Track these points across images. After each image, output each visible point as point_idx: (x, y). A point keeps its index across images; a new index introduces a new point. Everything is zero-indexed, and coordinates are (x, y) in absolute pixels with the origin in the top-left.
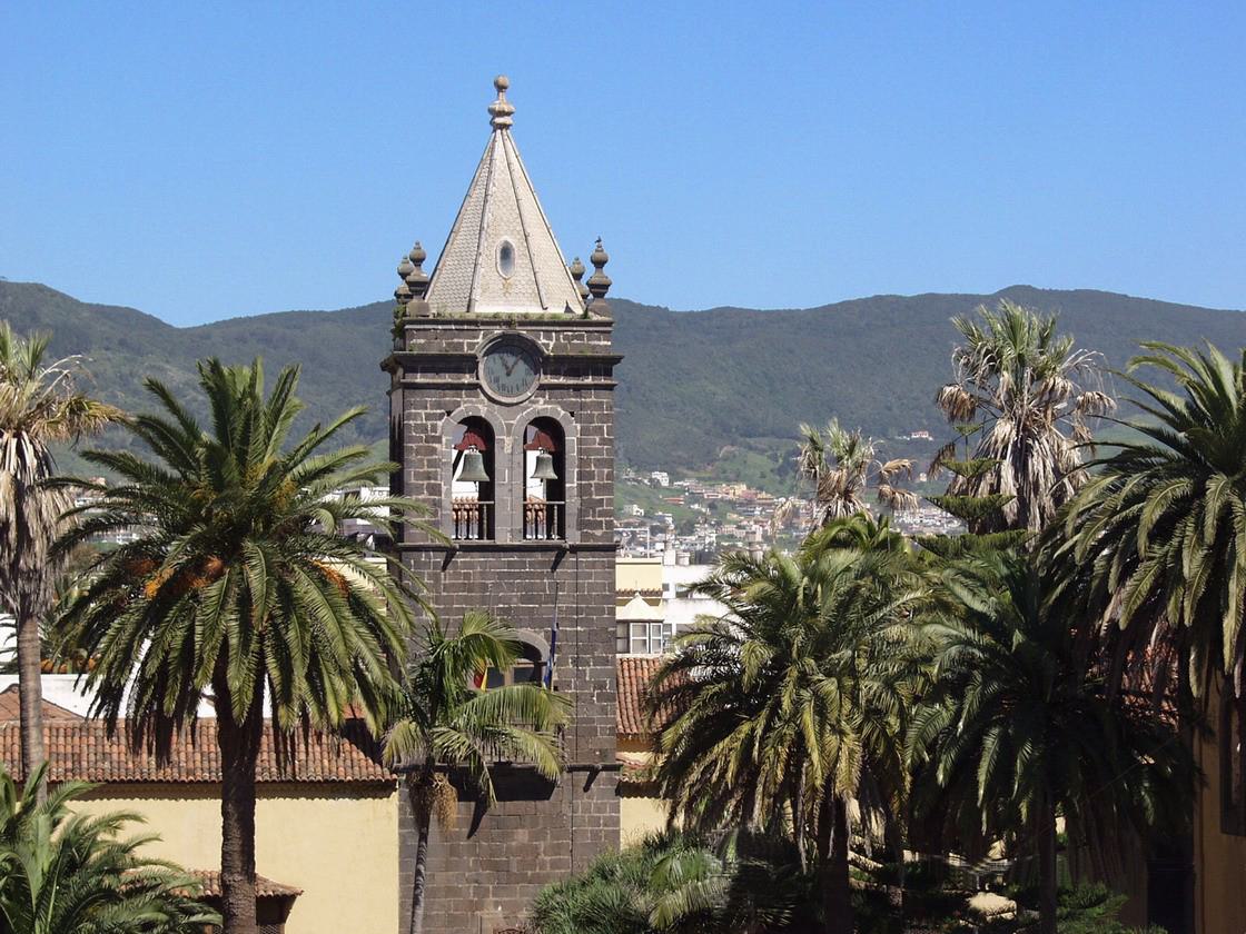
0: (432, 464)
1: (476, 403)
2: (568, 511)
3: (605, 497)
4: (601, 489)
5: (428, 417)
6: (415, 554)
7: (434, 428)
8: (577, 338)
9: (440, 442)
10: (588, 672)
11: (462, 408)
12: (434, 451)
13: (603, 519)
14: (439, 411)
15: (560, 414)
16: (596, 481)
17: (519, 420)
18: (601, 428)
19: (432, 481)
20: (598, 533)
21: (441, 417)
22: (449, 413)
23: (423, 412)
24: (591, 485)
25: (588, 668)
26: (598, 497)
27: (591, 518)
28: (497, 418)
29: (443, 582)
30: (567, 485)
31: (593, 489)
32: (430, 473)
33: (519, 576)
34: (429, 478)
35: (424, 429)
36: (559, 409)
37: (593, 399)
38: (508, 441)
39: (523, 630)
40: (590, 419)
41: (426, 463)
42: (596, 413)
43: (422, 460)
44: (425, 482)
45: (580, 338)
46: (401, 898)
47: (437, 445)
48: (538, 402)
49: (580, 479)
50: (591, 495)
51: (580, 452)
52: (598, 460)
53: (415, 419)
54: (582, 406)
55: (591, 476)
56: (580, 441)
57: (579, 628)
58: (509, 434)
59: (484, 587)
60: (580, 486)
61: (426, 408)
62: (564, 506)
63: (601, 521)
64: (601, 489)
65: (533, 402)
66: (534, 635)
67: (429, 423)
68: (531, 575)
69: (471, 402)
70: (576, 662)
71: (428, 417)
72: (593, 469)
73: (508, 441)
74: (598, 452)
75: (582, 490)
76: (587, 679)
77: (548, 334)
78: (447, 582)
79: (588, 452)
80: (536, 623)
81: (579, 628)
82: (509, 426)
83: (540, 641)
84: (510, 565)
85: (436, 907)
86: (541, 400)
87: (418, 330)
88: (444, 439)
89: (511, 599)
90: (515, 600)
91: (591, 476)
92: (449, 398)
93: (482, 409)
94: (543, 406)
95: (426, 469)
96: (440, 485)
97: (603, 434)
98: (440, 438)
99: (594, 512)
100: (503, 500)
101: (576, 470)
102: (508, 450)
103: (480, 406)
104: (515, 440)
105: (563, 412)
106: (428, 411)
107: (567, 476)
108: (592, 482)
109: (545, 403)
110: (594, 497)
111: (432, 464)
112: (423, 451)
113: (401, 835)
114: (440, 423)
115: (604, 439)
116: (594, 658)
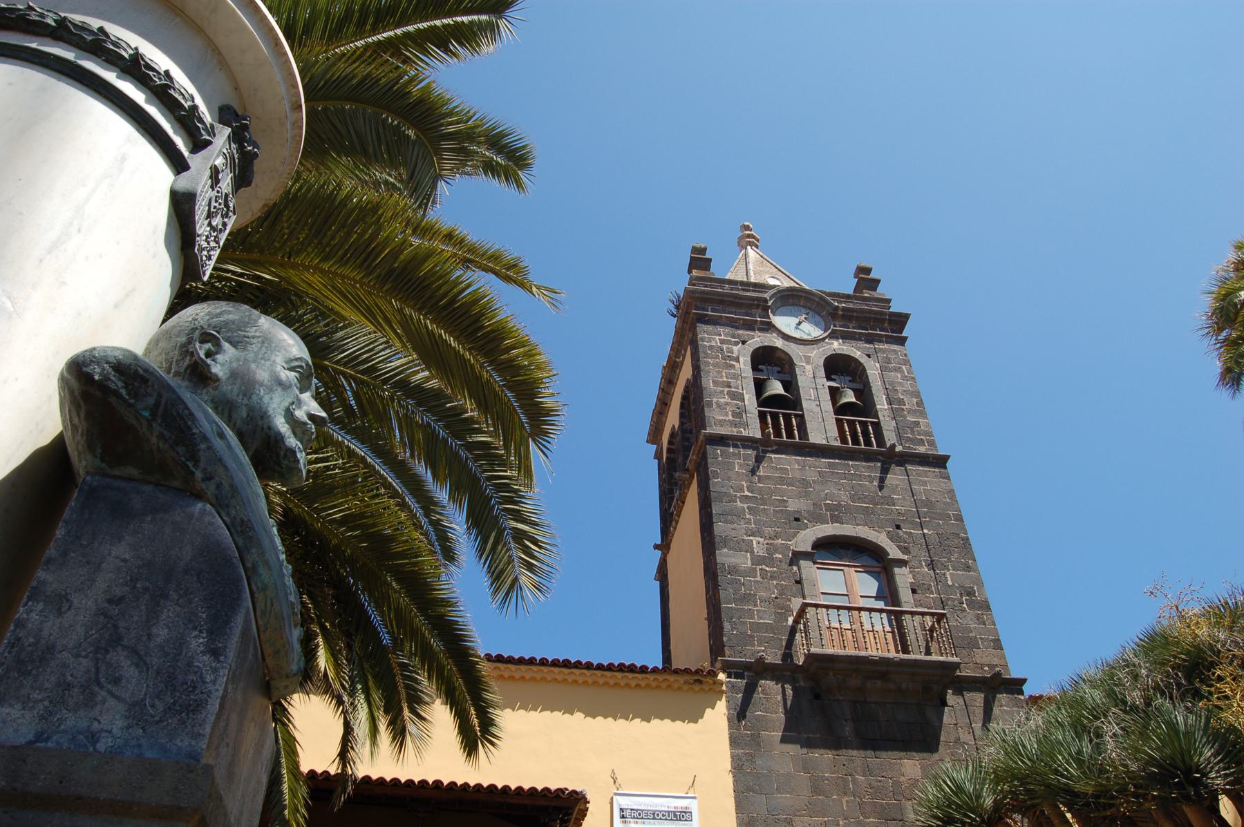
5: (722, 342)
15: (857, 354)
17: (818, 355)
21: (736, 344)
22: (744, 342)
28: (794, 350)
33: (845, 476)
34: (730, 387)
38: (809, 368)
49: (890, 403)
55: (901, 402)
58: (808, 363)
59: (805, 483)
70: (932, 565)
75: (895, 414)
79: (892, 383)
83: (881, 539)
88: (741, 359)
93: (779, 343)
94: (837, 346)
114: (735, 349)
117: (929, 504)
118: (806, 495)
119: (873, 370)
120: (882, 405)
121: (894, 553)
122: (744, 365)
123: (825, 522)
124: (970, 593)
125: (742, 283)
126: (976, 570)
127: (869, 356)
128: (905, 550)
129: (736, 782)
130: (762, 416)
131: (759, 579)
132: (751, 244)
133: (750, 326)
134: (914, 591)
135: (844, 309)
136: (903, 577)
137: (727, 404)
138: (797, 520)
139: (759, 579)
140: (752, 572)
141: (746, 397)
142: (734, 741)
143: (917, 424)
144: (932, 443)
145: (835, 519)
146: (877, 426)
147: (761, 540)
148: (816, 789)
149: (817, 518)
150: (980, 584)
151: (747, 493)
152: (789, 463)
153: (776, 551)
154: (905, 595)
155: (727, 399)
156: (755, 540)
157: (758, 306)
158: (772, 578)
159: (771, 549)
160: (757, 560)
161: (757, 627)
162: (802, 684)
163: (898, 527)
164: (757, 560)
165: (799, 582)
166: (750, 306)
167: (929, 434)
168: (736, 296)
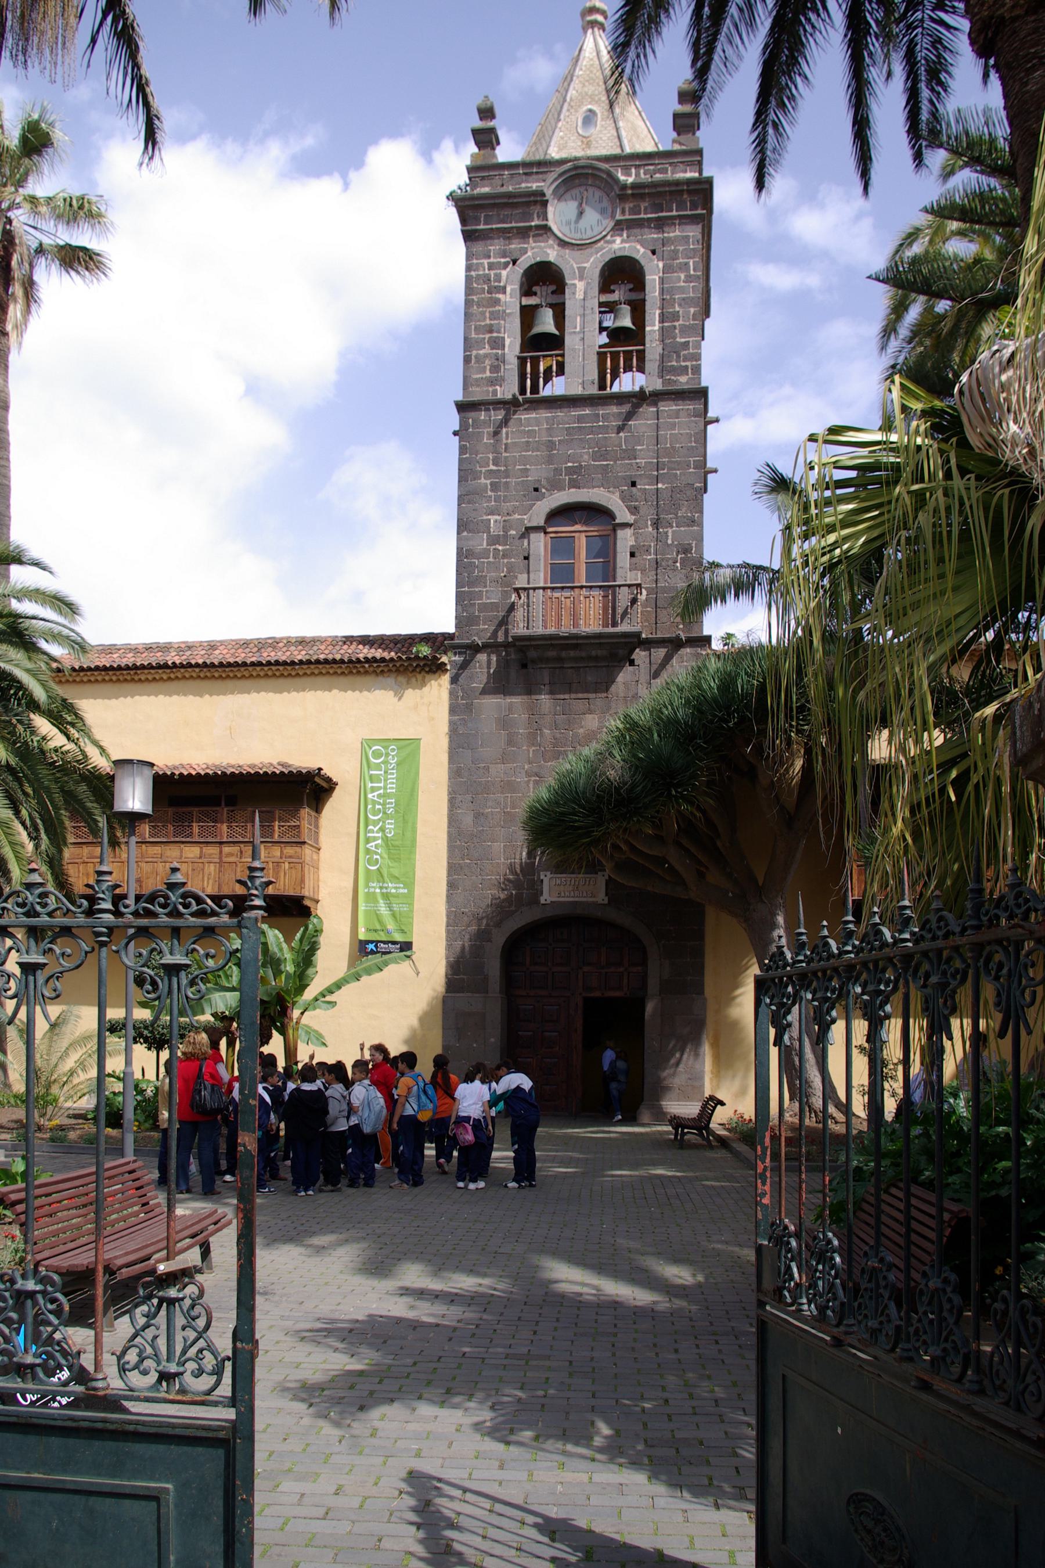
0: (494, 316)
1: (545, 247)
2: (648, 356)
3: (691, 339)
4: (685, 330)
6: (473, 414)
7: (498, 278)
8: (660, 171)
9: (505, 293)
10: (670, 534)
11: (529, 254)
12: (497, 302)
13: (688, 364)
14: (503, 260)
15: (639, 252)
16: (681, 322)
17: (594, 262)
18: (687, 264)
19: (495, 335)
20: (683, 379)
21: (506, 265)
22: (514, 262)
23: (485, 262)
24: (675, 327)
25: (670, 531)
26: (683, 340)
27: (674, 363)
29: (504, 441)
30: (648, 329)
31: (677, 331)
32: (491, 325)
34: (491, 331)
35: (487, 279)
36: (639, 247)
37: (677, 233)
38: (580, 286)
39: (596, 490)
40: (674, 256)
41: (488, 315)
42: (681, 248)
43: (483, 313)
44: (487, 336)
45: (665, 171)
46: (450, 793)
47: (501, 296)
48: (614, 241)
49: (662, 321)
50: (675, 338)
51: (662, 291)
52: (684, 299)
53: (477, 270)
54: (664, 242)
55: (675, 317)
56: (662, 281)
57: (660, 485)
58: (581, 278)
59: (551, 445)
60: (662, 329)
61: (489, 257)
62: (644, 351)
63: (686, 367)
64: (685, 330)
65: (608, 242)
66: (607, 494)
67: (492, 273)
68: (605, 429)
69: (540, 247)
70: (656, 524)
71: (491, 267)
72: (677, 309)
73: (580, 286)
74: (682, 290)
76: (670, 542)
77: (626, 171)
78: (509, 441)
79: (672, 291)
80: (607, 483)
81: (660, 485)
82: (581, 270)
84: (580, 419)
85: (489, 804)
86: (618, 240)
87: (483, 178)
88: (508, 289)
89: (582, 456)
90: (586, 457)
91: (675, 317)
92: (515, 246)
93: (552, 254)
94: (619, 245)
95: (488, 322)
96: (503, 338)
97: (688, 270)
98: (505, 288)
99: (678, 356)
100: (574, 350)
101: (658, 312)
102: (580, 295)
103: (549, 251)
104: (588, 283)
105: (642, 250)
106: (492, 260)
107: (647, 318)
108: (677, 324)
109: (623, 242)
110: (678, 340)
111: (494, 316)
112: (484, 303)
113: (451, 722)
114: (504, 273)
115: (690, 276)
116: (677, 517)
117: (671, 452)
118: (550, 460)
119: (653, 279)
120: (653, 327)
121: (623, 515)
122: (511, 300)
123: (561, 489)
124: (686, 550)
125: (524, 164)
126: (700, 525)
127: (654, 252)
128: (634, 510)
129: (450, 742)
130: (522, 361)
131: (491, 559)
132: (593, 24)
133: (524, 233)
134: (632, 555)
135: (634, 186)
136: (626, 539)
137: (486, 356)
138: (536, 490)
139: (491, 559)
140: (485, 554)
141: (507, 342)
142: (453, 710)
143: (686, 345)
144: (697, 370)
145: (574, 484)
146: (641, 356)
147: (498, 518)
148: (510, 742)
149: (556, 485)
150: (700, 539)
151: (492, 467)
152: (538, 422)
153: (511, 528)
154: (623, 559)
155: (487, 350)
156: (493, 518)
157: (535, 202)
158: (504, 556)
159: (506, 526)
160: (494, 540)
161: (484, 607)
162: (513, 656)
163: (634, 484)
164: (494, 540)
165: (526, 558)
166: (528, 204)
167: (697, 357)
168: (509, 195)
